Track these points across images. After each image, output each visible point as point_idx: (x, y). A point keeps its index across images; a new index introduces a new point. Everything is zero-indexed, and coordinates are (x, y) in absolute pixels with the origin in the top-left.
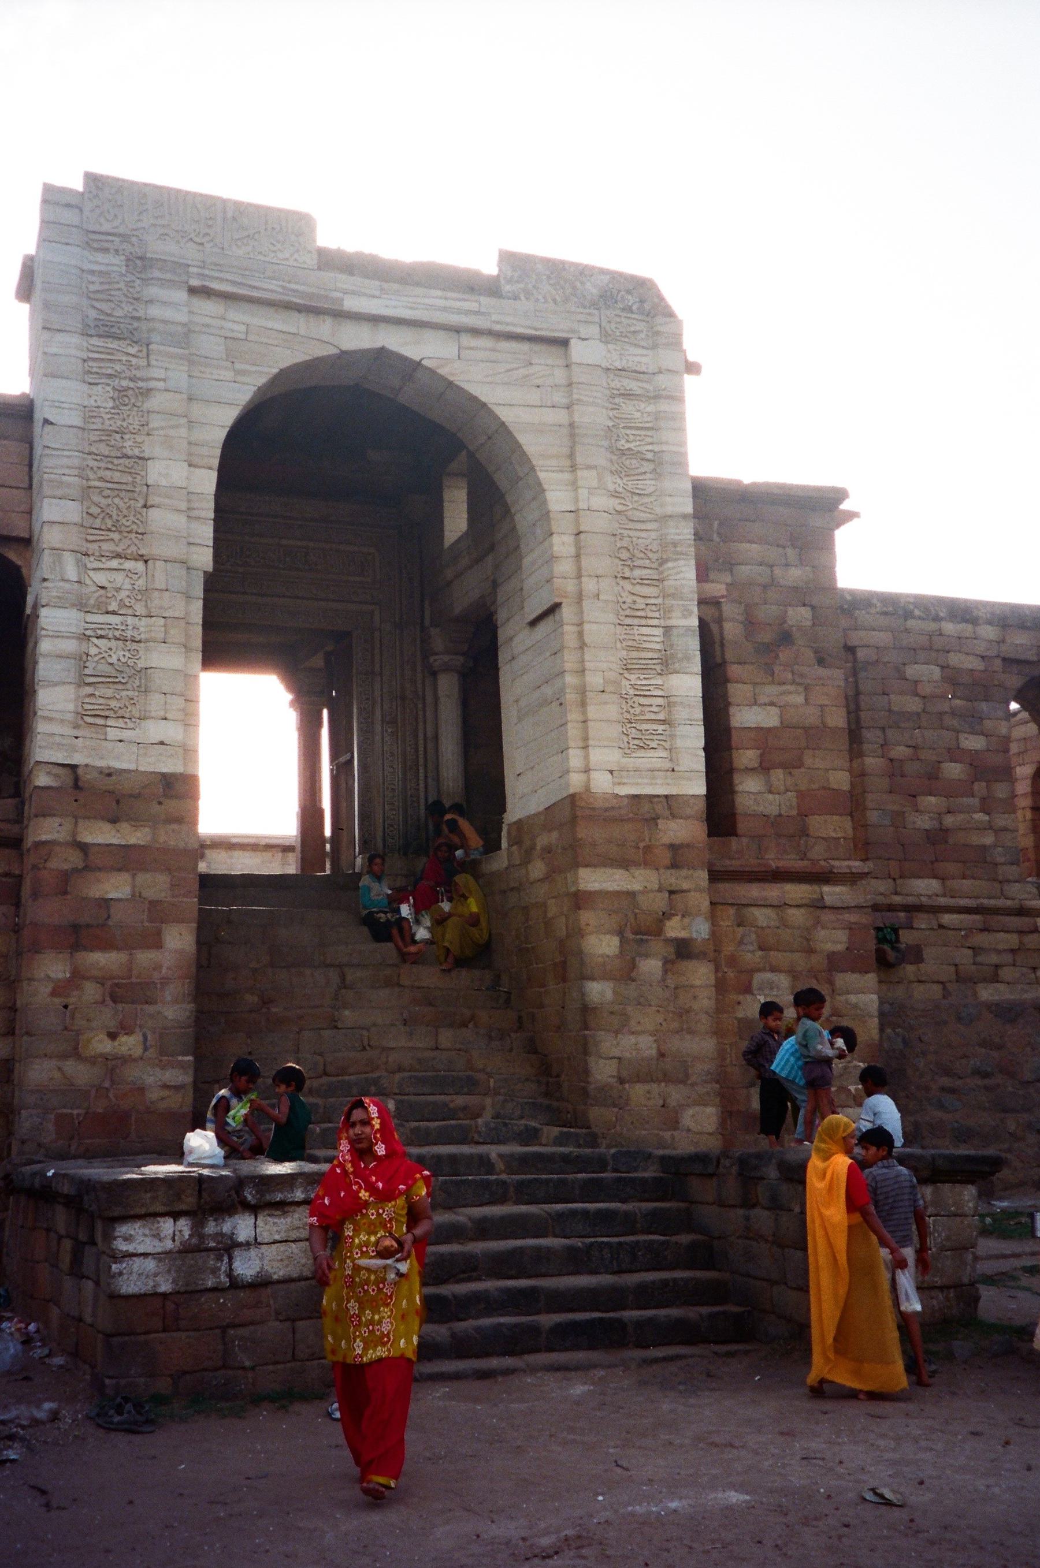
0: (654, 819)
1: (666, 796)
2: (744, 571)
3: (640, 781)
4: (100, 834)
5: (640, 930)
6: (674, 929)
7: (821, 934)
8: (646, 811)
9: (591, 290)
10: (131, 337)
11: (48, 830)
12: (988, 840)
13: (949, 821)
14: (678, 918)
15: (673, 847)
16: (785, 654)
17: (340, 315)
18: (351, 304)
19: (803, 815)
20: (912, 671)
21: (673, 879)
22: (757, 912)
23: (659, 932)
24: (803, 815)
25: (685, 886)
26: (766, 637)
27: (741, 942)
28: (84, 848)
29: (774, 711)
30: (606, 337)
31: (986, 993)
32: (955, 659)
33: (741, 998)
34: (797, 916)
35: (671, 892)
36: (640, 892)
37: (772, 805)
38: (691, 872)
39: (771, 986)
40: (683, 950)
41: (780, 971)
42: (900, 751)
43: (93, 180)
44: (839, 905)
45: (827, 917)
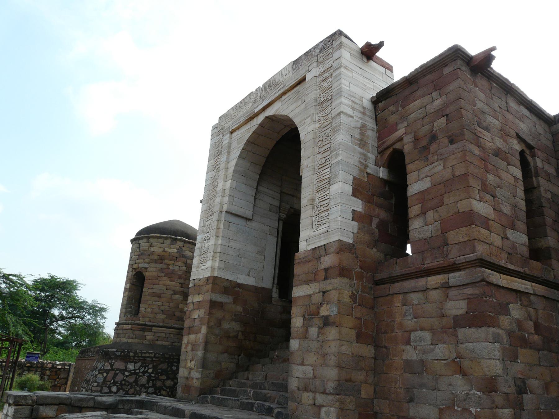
1: (324, 245)
3: (315, 241)
5: (310, 315)
6: (324, 312)
7: (449, 304)
9: (317, 51)
14: (325, 305)
15: (326, 270)
18: (257, 110)
19: (444, 232)
21: (326, 286)
22: (413, 296)
23: (318, 313)
24: (444, 232)
25: (329, 288)
26: (424, 143)
27: (405, 315)
29: (428, 179)
30: (319, 63)
33: (405, 347)
34: (435, 295)
35: (324, 293)
36: (312, 294)
38: (332, 280)
39: (421, 339)
40: (326, 322)
41: (425, 330)
44: (458, 284)
45: (453, 293)
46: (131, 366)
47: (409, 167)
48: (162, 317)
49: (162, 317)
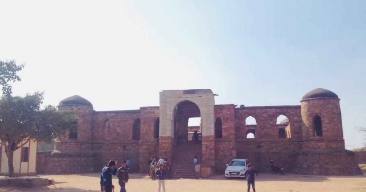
0: (209, 138)
2: (223, 113)
4: (164, 141)
6: (211, 147)
8: (208, 137)
10: (166, 102)
11: (160, 141)
12: (272, 133)
13: (268, 132)
15: (211, 140)
16: (228, 121)
17: (182, 98)
20: (263, 115)
28: (162, 142)
31: (271, 151)
32: (270, 113)
37: (226, 135)
40: (211, 149)
42: (262, 124)
43: (163, 91)
46: (83, 159)
47: (222, 123)
48: (86, 139)
49: (86, 139)
